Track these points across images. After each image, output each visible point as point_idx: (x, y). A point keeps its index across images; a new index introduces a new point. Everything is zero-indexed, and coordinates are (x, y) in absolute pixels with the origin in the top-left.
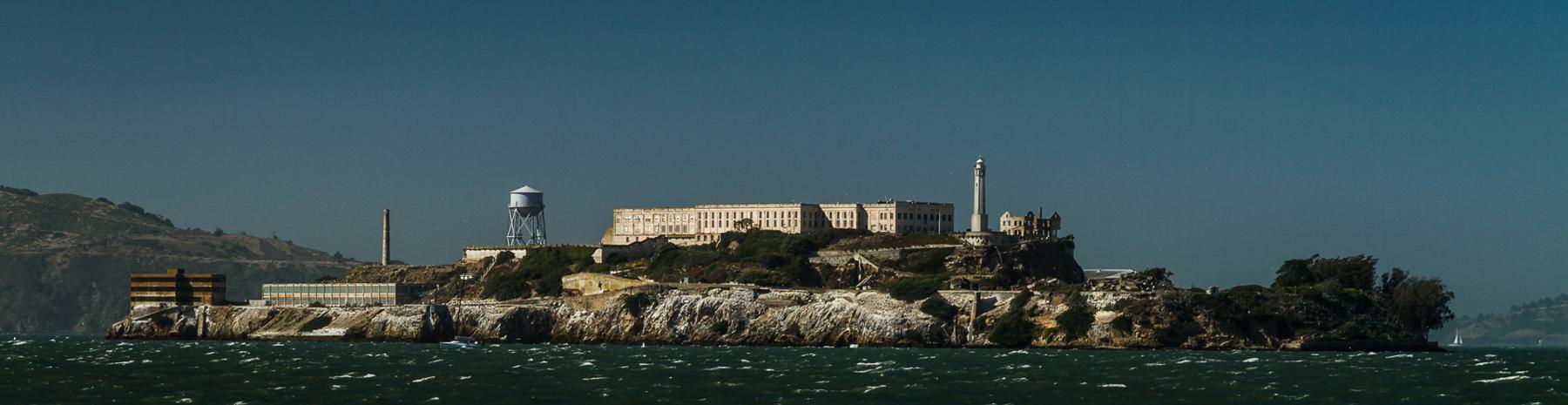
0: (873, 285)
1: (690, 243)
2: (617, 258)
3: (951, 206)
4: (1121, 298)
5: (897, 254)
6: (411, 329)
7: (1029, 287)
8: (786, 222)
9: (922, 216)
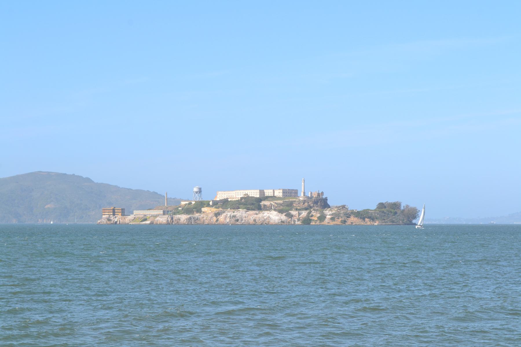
0: (275, 210)
1: (234, 200)
2: (216, 204)
3: (297, 190)
4: (333, 212)
6: (164, 221)
7: (312, 210)
9: (289, 193)
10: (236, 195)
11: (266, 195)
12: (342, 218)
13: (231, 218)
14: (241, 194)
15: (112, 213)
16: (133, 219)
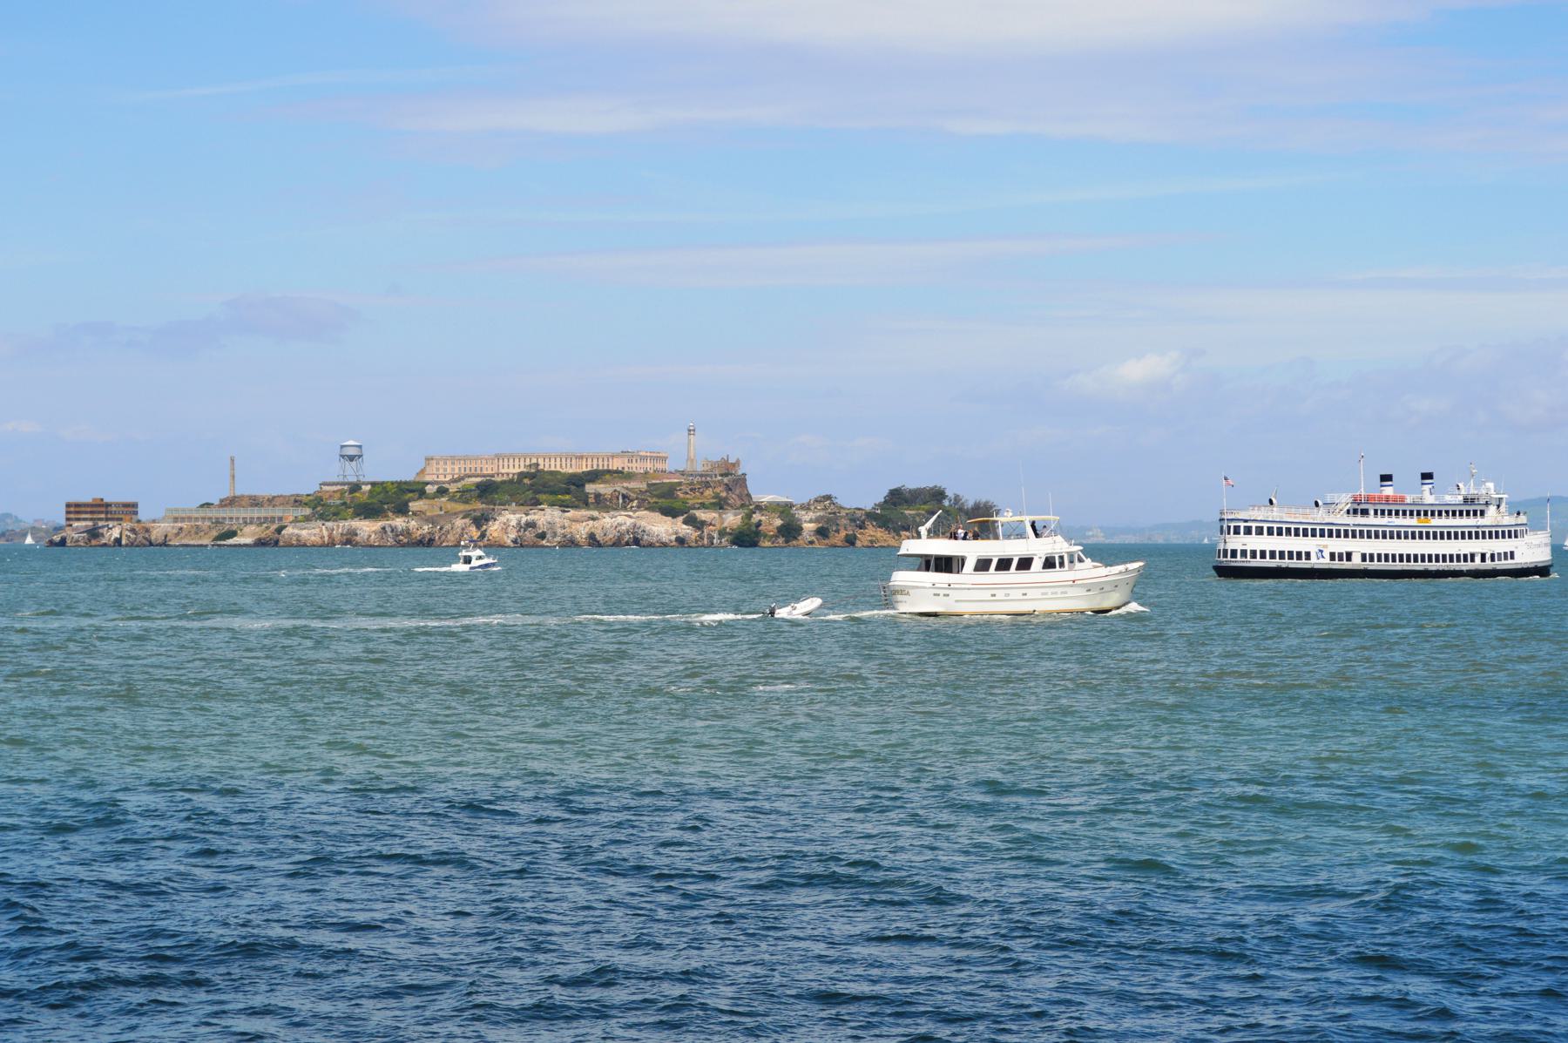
6: (313, 538)
8: (564, 465)
10: (501, 467)
12: (846, 529)
16: (175, 531)
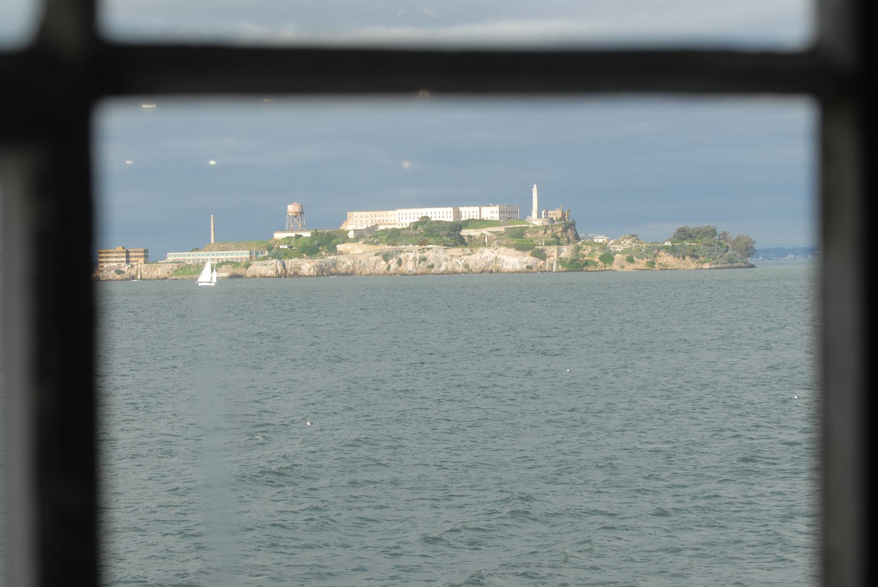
0: (500, 245)
5: (503, 230)
6: (270, 272)
7: (579, 243)
8: (445, 216)
10: (401, 218)
11: (463, 219)
13: (417, 262)
14: (412, 216)
15: (124, 259)
